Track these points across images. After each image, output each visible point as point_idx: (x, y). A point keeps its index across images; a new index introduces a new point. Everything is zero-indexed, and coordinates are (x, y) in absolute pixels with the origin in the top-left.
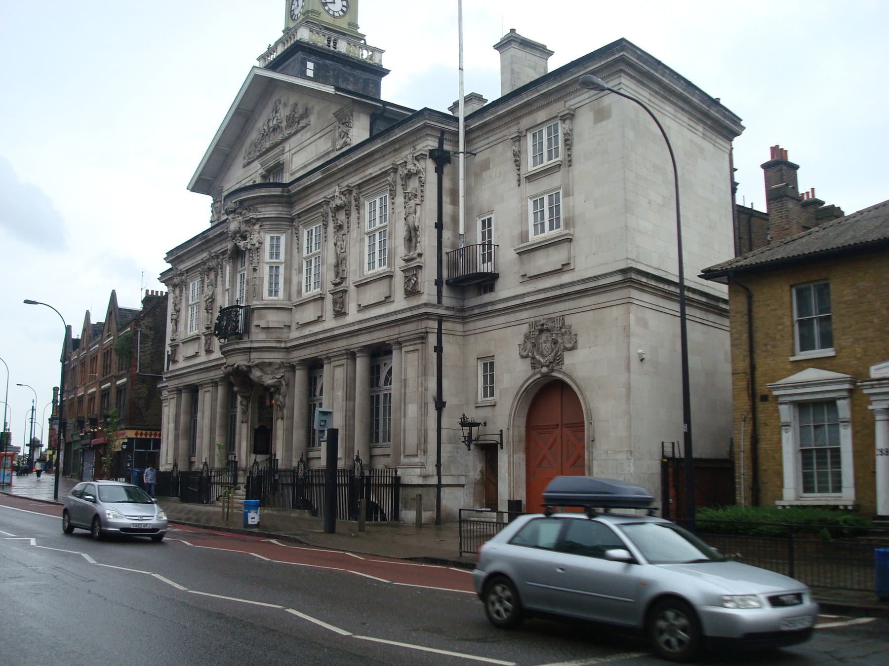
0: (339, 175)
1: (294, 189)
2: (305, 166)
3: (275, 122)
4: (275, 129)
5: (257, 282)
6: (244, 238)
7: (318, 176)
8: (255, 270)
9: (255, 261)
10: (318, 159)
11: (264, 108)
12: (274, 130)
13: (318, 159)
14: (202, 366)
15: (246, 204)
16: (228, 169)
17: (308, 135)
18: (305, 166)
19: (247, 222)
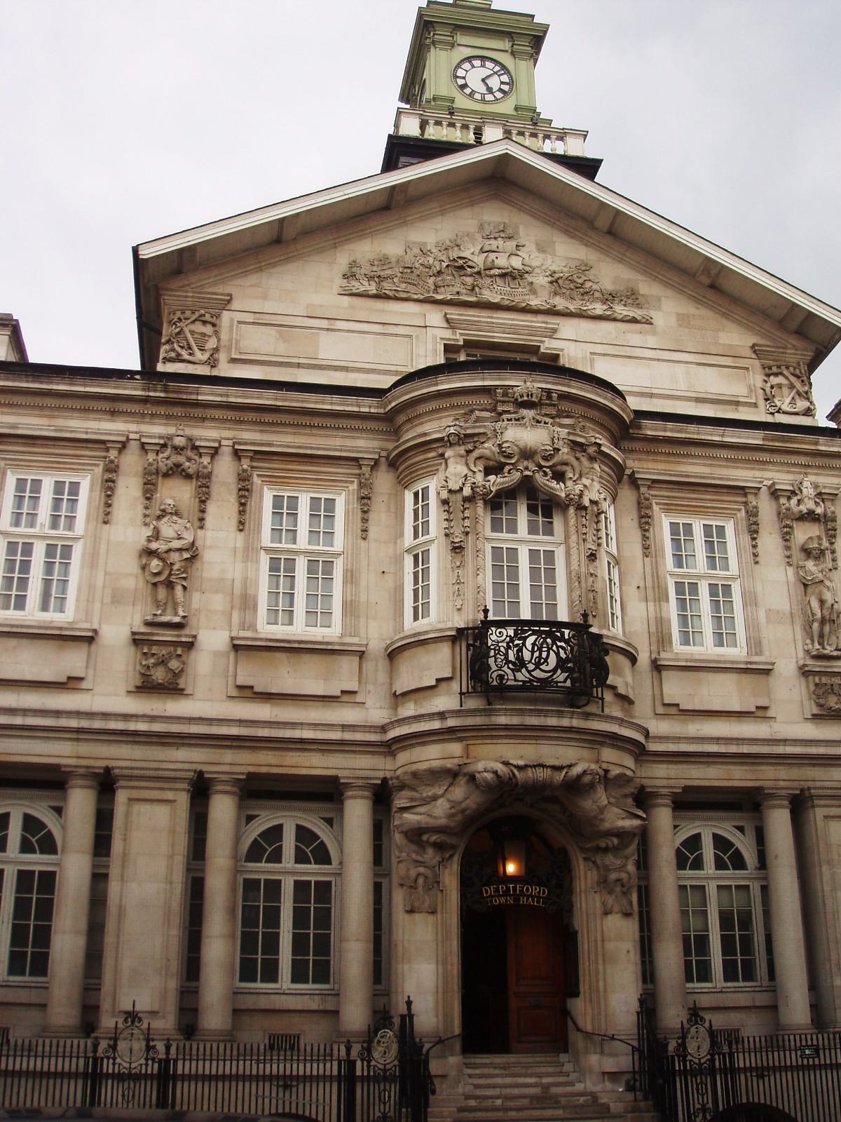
0: (803, 460)
1: (651, 429)
2: (652, 395)
3: (516, 263)
4: (510, 275)
5: (598, 586)
6: (559, 477)
7: (755, 438)
8: (592, 557)
9: (590, 537)
10: (698, 400)
11: (443, 213)
12: (503, 276)
13: (698, 400)
14: (142, 726)
15: (565, 406)
16: (260, 269)
17: (651, 341)
18: (652, 395)
19: (576, 446)
